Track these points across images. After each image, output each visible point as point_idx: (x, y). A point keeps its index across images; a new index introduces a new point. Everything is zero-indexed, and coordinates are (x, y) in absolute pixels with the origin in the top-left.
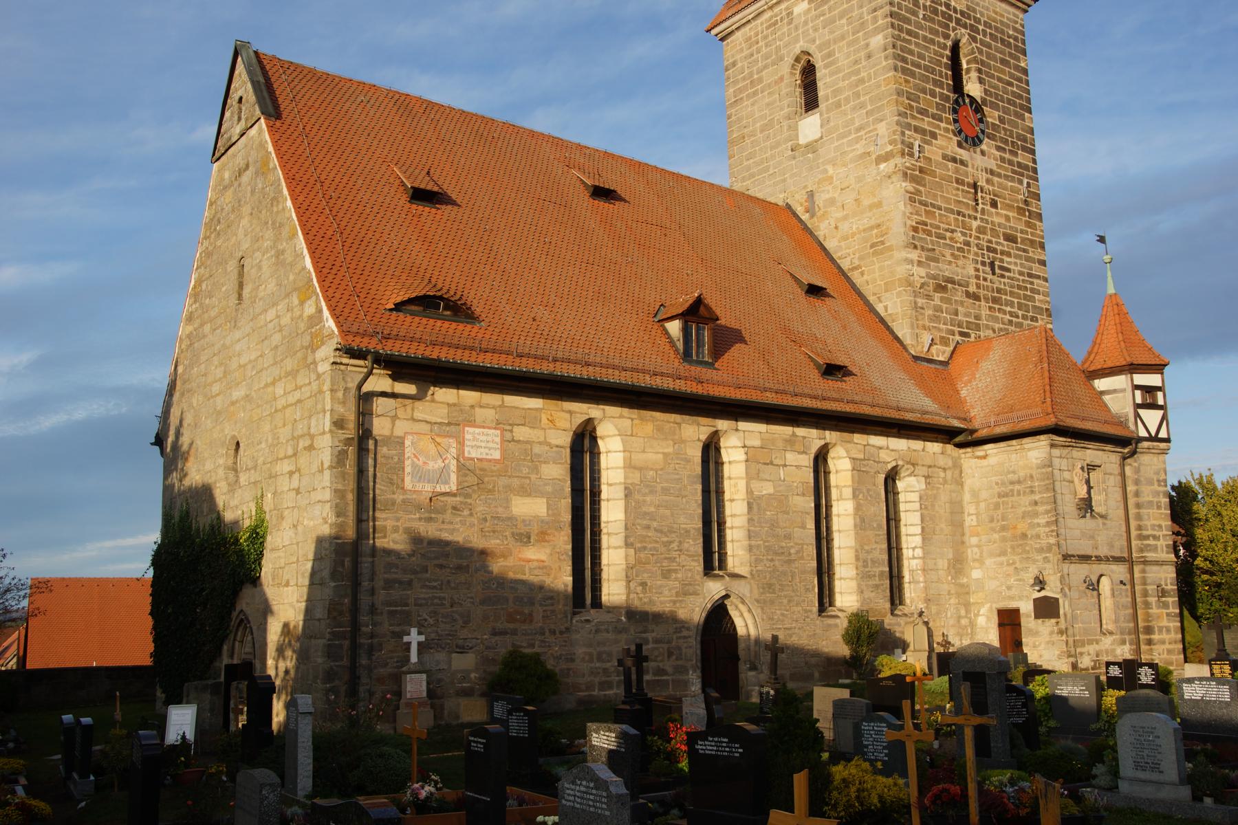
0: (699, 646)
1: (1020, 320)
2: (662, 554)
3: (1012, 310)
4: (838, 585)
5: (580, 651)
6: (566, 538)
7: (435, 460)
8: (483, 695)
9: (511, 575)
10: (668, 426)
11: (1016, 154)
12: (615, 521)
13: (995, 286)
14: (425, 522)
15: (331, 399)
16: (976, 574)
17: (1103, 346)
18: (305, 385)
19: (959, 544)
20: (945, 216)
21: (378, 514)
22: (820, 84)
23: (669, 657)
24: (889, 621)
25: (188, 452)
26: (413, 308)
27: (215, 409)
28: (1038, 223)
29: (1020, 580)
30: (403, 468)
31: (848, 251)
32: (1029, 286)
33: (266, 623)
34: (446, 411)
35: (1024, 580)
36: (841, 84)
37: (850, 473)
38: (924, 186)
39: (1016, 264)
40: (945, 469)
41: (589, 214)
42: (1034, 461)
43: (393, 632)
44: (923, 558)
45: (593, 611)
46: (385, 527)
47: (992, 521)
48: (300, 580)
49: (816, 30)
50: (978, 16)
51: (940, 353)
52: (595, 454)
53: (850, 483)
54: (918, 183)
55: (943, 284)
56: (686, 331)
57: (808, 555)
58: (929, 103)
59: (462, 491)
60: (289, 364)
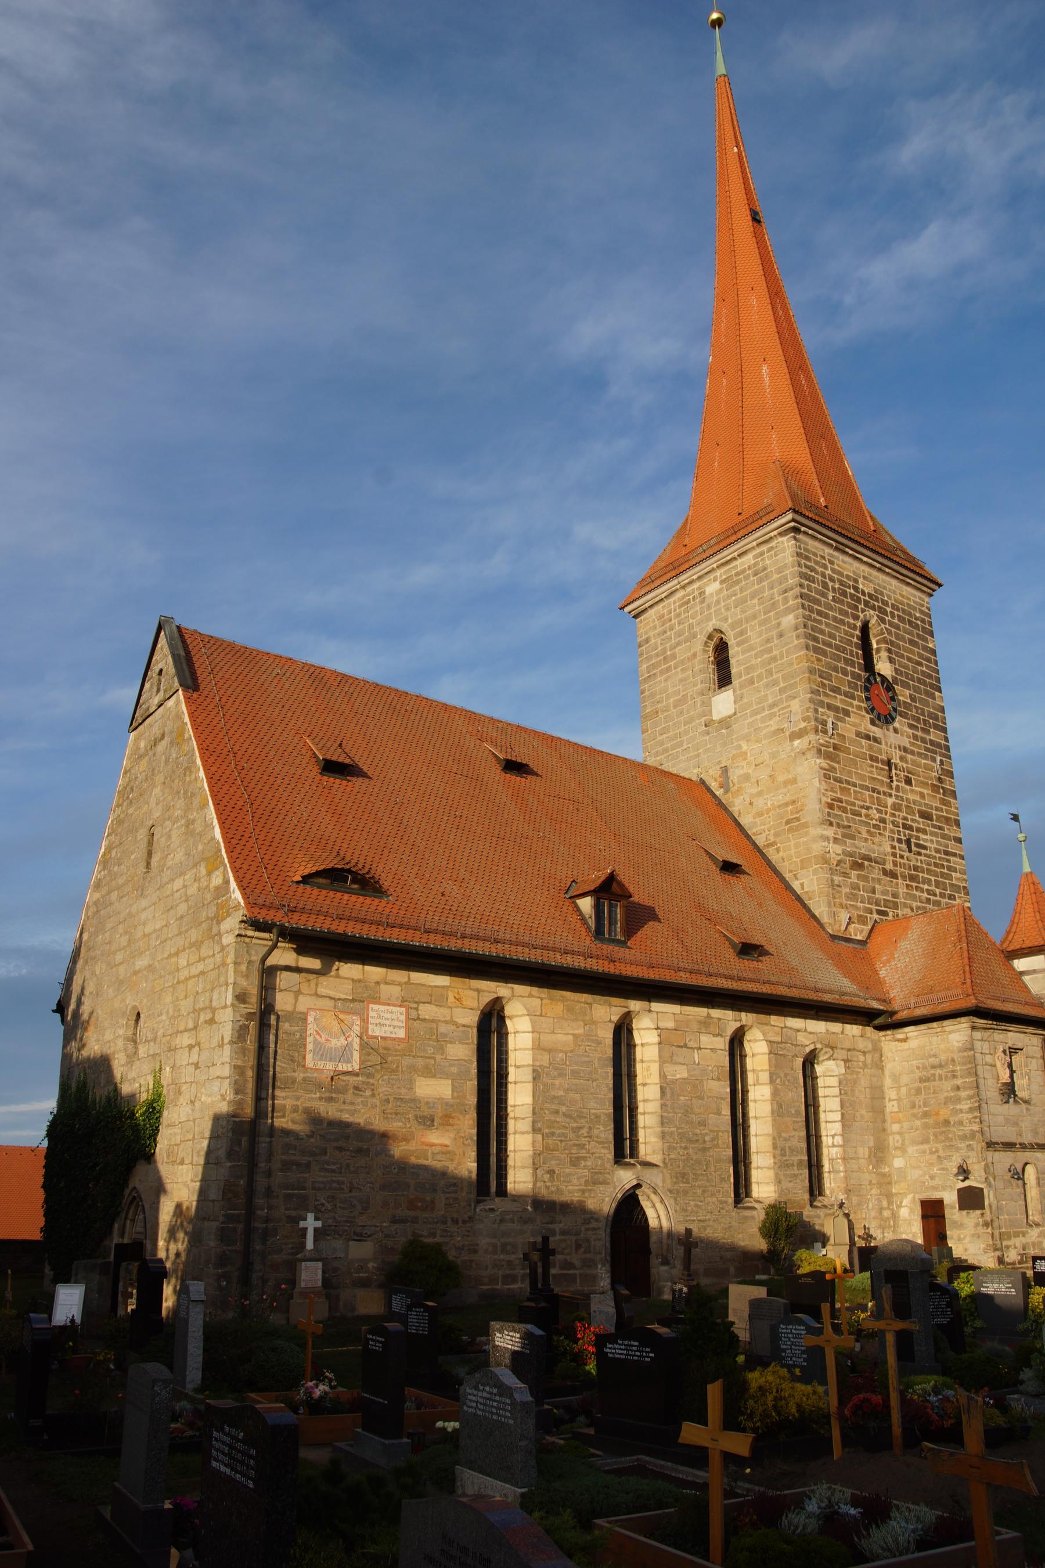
0: (608, 1239)
1: (938, 898)
2: (571, 1140)
3: (930, 888)
4: (755, 1175)
5: (484, 1241)
6: (471, 1122)
7: (338, 1038)
8: (380, 1286)
9: (413, 1160)
10: (578, 1006)
11: (928, 732)
12: (522, 1105)
13: (912, 864)
14: (325, 1101)
15: (234, 972)
16: (898, 1163)
17: (1021, 925)
18: (209, 957)
19: (880, 1131)
20: (860, 793)
21: (278, 1093)
22: (733, 661)
24: (808, 1213)
25: (88, 1022)
26: (321, 880)
27: (117, 978)
28: (952, 801)
29: (943, 1169)
30: (305, 1045)
31: (763, 827)
32: (945, 864)
33: (158, 1202)
34: (351, 987)
35: (947, 1169)
36: (753, 662)
37: (767, 1056)
38: (838, 762)
39: (932, 841)
40: (864, 1053)
41: (500, 788)
42: (956, 1044)
43: (289, 1217)
44: (843, 1146)
45: (497, 1200)
46: (285, 1106)
47: (913, 1106)
48: (195, 1158)
49: (728, 609)
50: (886, 599)
51: (858, 932)
52: (503, 1035)
53: (767, 1067)
54: (833, 760)
55: (860, 861)
56: (598, 908)
57: (724, 1143)
58: (841, 681)
59: (364, 1070)
60: (194, 935)
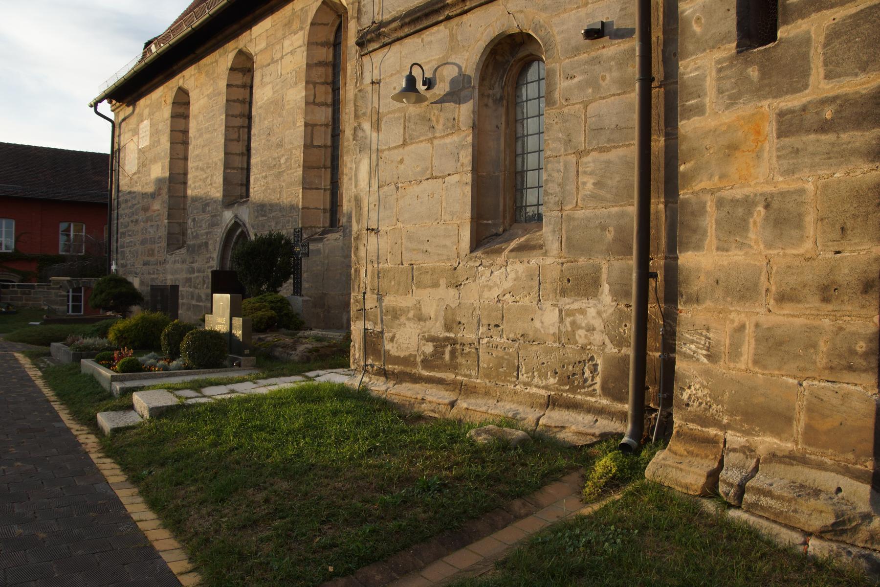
23: (204, 284)
